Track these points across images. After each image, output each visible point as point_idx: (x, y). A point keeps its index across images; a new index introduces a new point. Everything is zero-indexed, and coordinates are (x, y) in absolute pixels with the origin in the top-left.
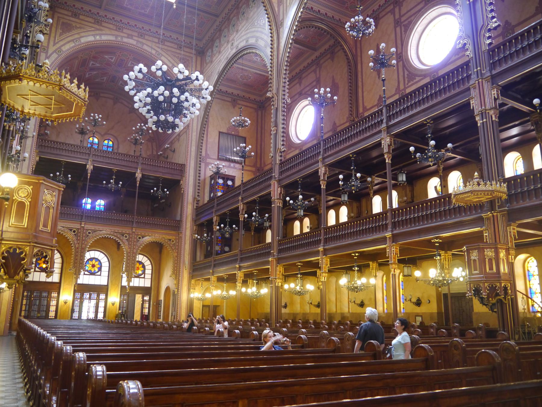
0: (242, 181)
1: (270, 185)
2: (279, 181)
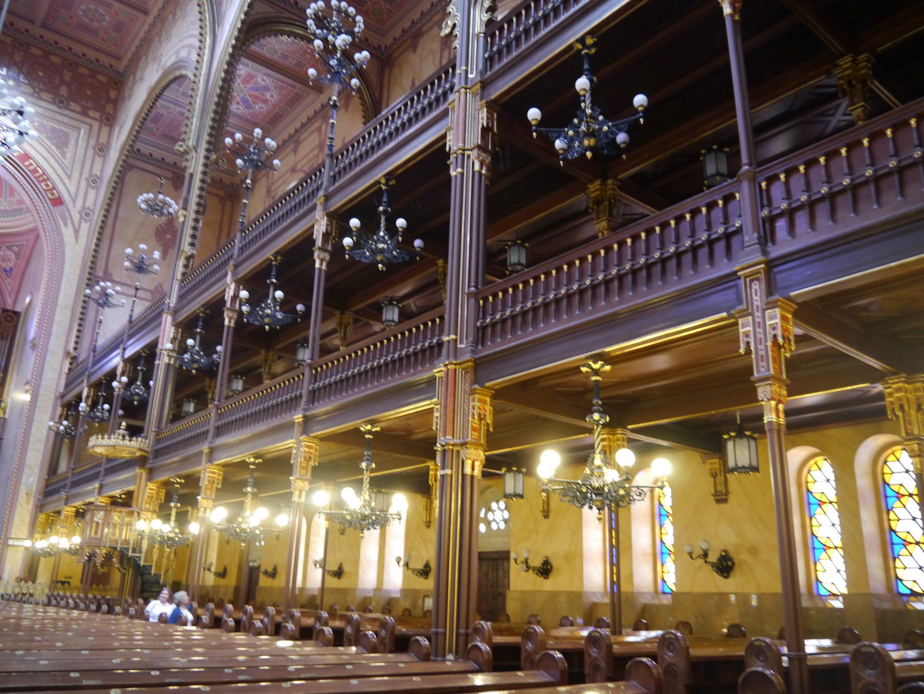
0: (131, 316)
1: (160, 324)
2: (175, 312)
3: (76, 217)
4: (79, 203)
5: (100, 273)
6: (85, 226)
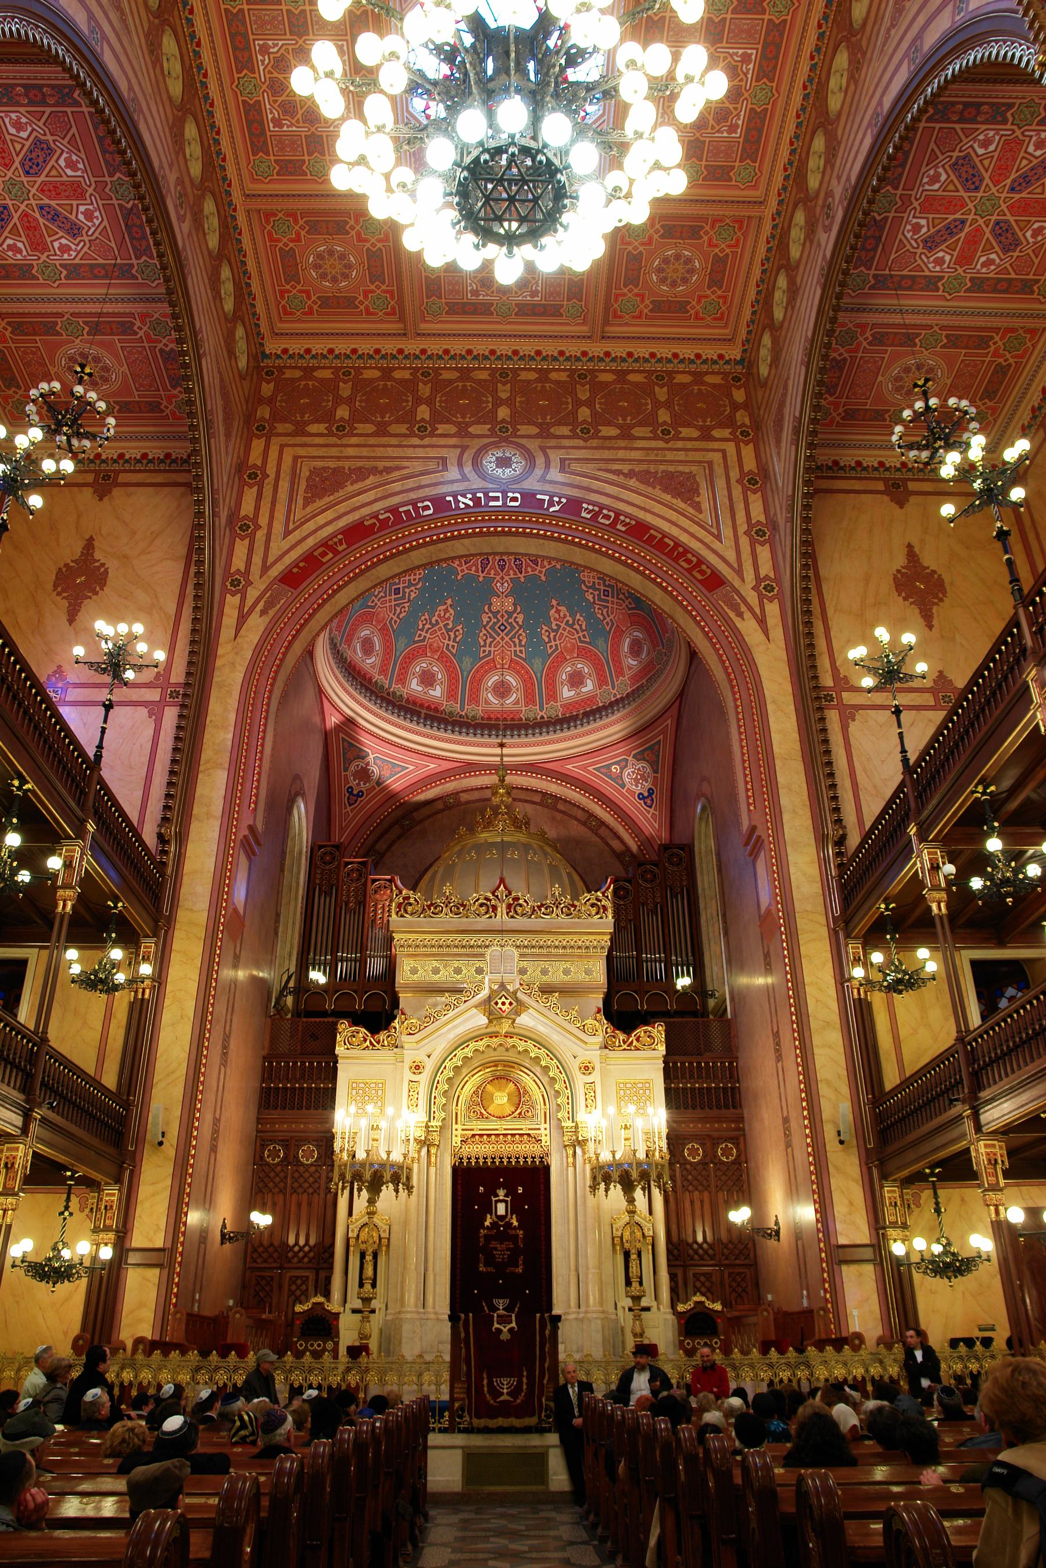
3: (752, 598)
5: (827, 681)
6: (773, 609)
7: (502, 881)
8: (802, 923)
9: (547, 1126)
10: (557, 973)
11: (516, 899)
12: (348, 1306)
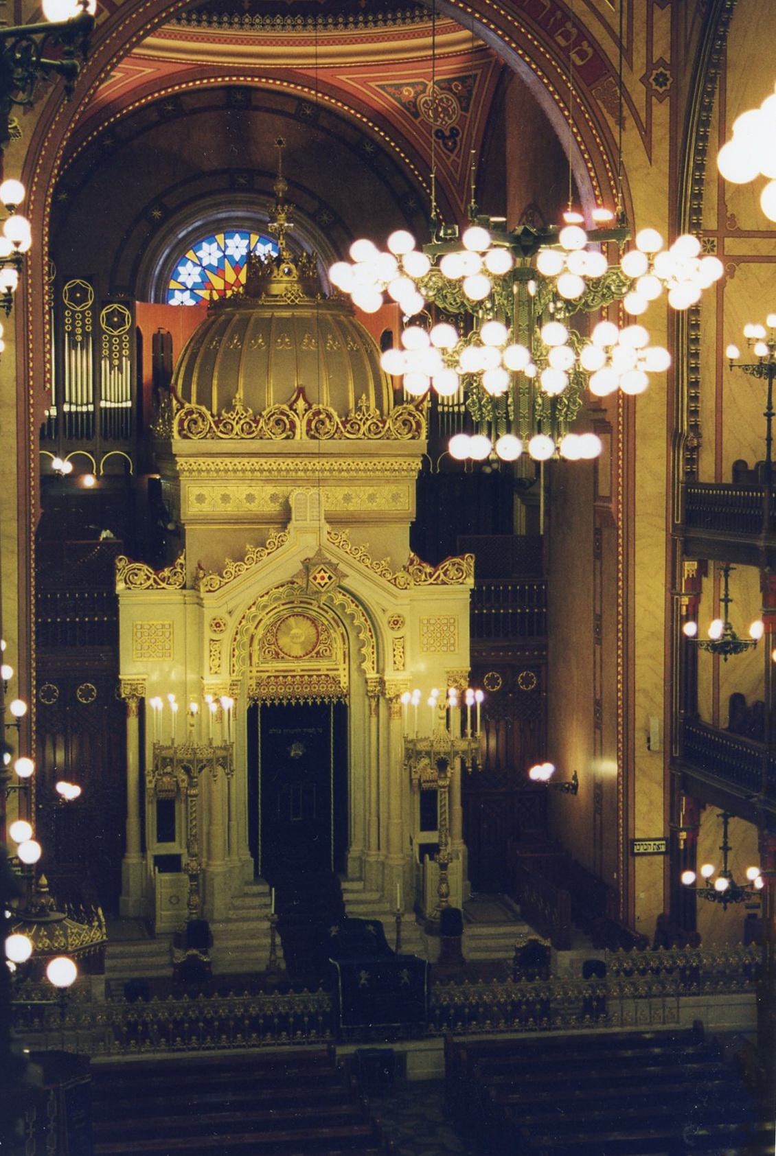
3: (638, 93)
4: (639, 60)
6: (661, 113)
7: (301, 391)
8: (641, 526)
9: (346, 666)
10: (361, 500)
11: (318, 413)
12: (150, 854)
